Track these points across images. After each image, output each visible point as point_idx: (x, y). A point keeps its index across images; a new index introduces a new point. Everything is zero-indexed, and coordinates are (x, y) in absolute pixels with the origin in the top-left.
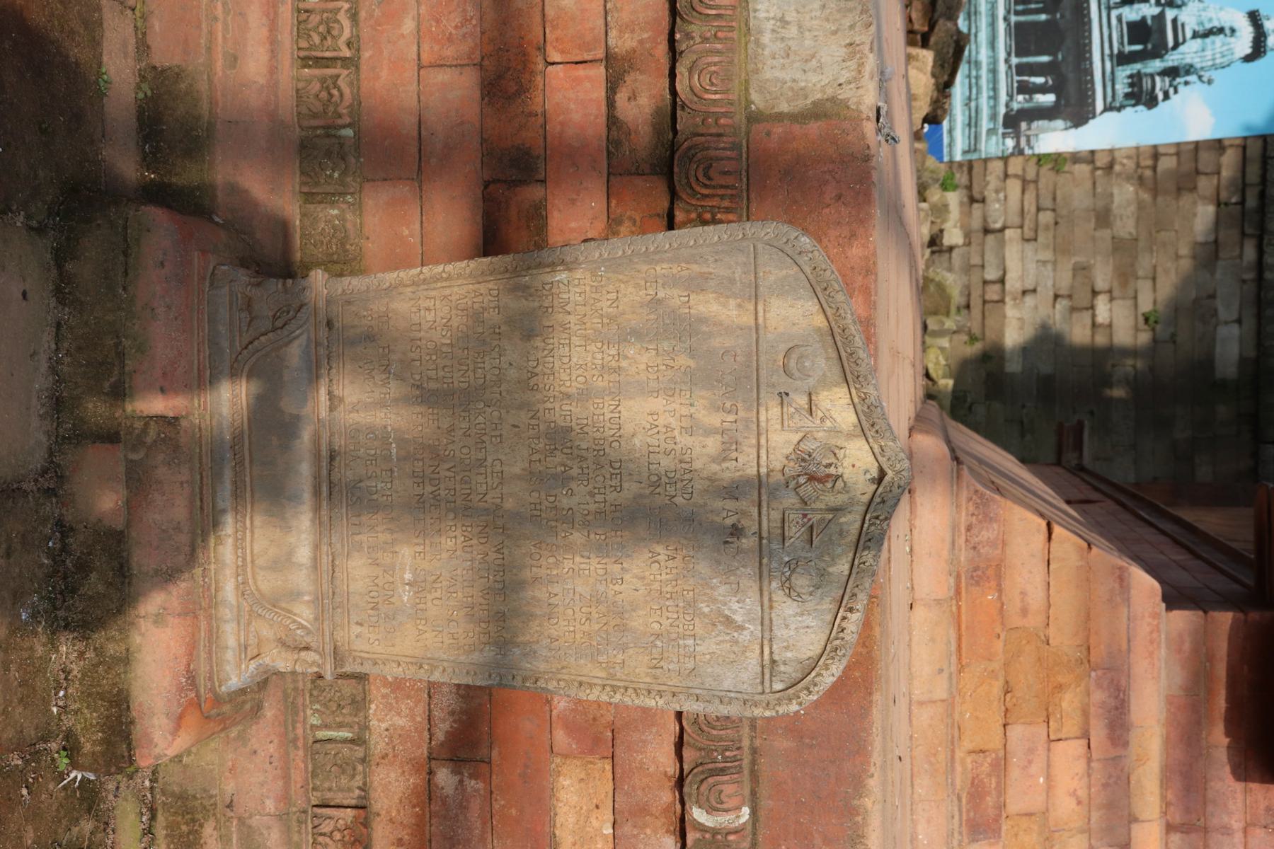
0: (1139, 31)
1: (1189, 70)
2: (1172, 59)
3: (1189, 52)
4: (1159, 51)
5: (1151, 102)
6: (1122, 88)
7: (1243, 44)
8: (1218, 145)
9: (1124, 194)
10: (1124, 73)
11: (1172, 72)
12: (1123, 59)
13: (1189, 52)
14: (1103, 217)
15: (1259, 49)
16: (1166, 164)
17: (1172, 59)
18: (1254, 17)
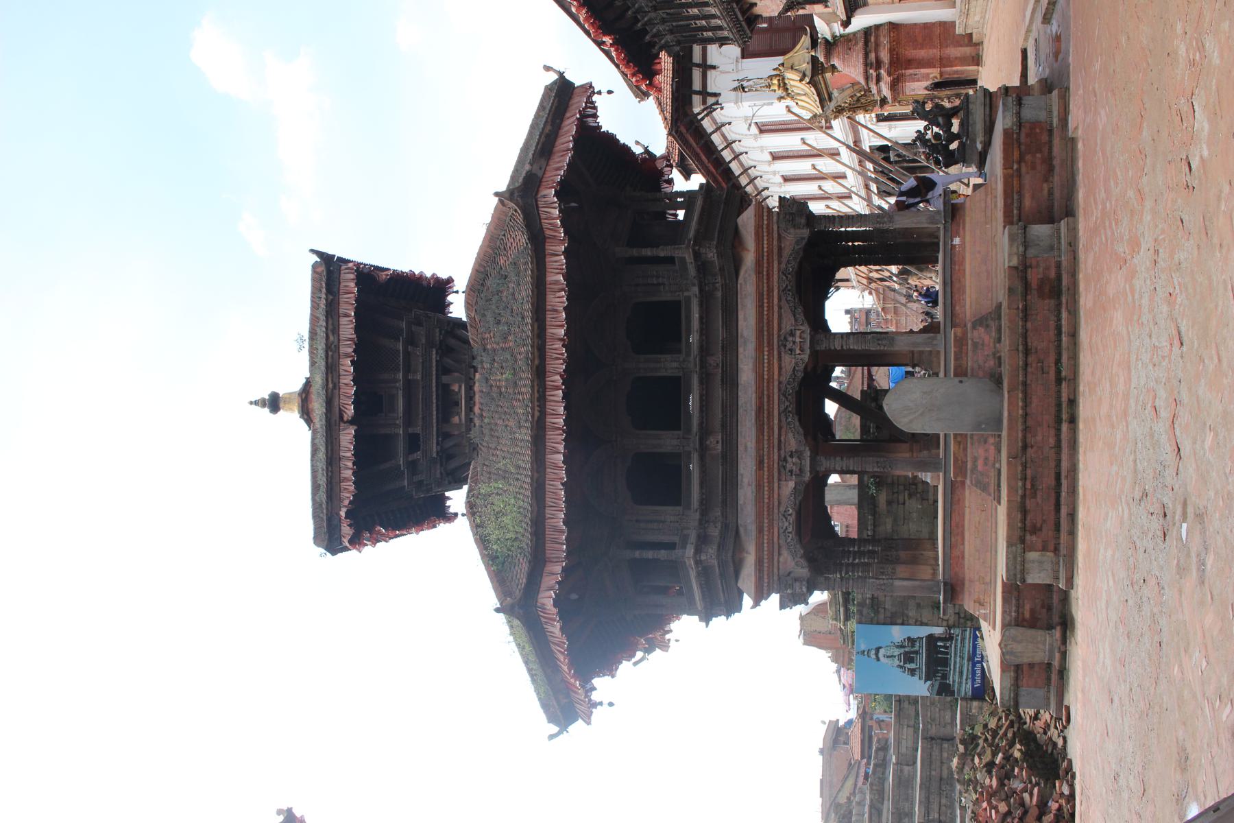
0: (911, 660)
2: (902, 650)
3: (896, 653)
4: (906, 653)
9: (912, 613)
10: (917, 648)
12: (916, 652)
13: (897, 652)
14: (918, 605)
16: (900, 621)
17: (902, 650)
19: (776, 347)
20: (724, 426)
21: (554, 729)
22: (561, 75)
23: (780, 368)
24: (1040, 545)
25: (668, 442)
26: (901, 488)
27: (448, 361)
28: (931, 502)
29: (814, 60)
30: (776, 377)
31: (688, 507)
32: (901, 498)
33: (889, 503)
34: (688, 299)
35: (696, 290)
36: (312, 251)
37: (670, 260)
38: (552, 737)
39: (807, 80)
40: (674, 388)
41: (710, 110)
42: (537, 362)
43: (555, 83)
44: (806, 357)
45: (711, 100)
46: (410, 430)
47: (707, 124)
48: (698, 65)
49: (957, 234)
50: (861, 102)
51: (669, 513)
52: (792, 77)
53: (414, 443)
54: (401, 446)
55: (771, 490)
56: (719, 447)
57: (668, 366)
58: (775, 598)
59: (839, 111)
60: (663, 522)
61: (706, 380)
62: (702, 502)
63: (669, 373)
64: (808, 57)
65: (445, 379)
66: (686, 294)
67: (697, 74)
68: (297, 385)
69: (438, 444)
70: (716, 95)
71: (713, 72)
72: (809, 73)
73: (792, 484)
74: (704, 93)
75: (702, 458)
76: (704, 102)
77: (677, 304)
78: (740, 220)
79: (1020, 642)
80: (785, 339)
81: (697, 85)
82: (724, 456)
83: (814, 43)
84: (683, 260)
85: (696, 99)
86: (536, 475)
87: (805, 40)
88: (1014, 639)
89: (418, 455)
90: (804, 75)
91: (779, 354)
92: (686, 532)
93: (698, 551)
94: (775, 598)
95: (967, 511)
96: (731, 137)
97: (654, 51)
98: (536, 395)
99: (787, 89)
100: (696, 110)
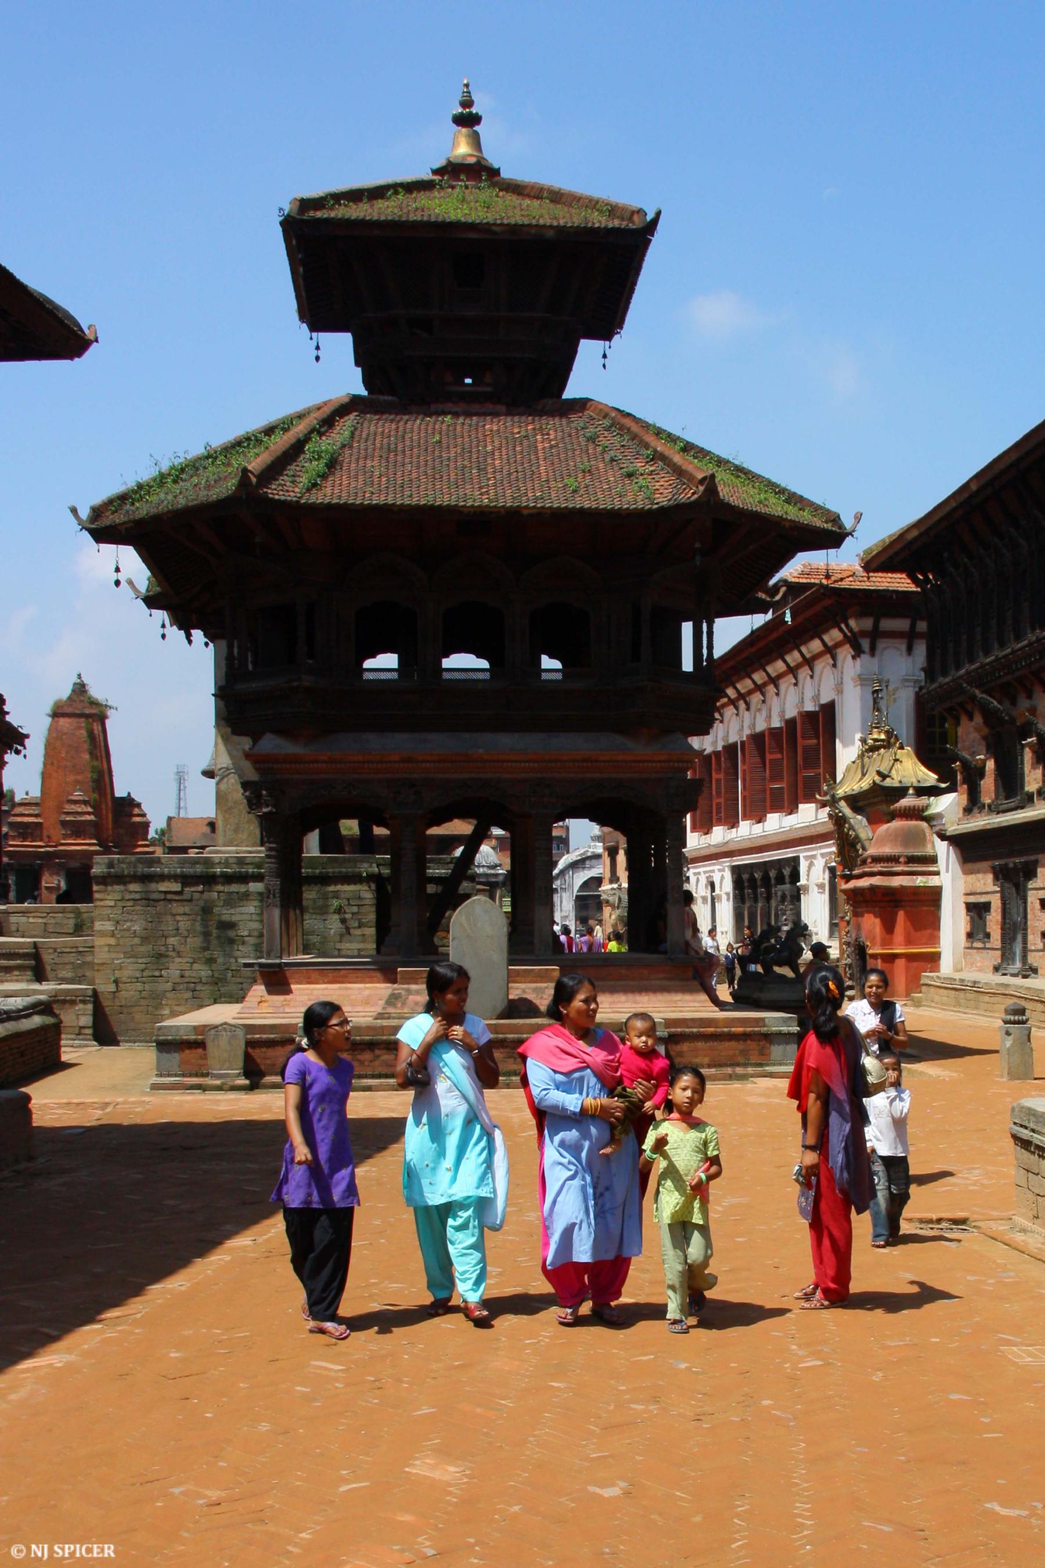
21: (84, 513)
22: (851, 534)
36: (658, 214)
38: (74, 511)
41: (854, 641)
43: (841, 526)
45: (865, 644)
47: (834, 635)
50: (849, 850)
52: (882, 760)
58: (253, 776)
59: (839, 821)
64: (907, 782)
67: (901, 624)
68: (493, 157)
70: (873, 652)
71: (904, 647)
72: (888, 783)
74: (875, 635)
76: (863, 634)
81: (887, 624)
83: (923, 791)
85: (868, 623)
87: (931, 778)
90: (884, 776)
96: (819, 665)
99: (873, 749)
100: (852, 623)
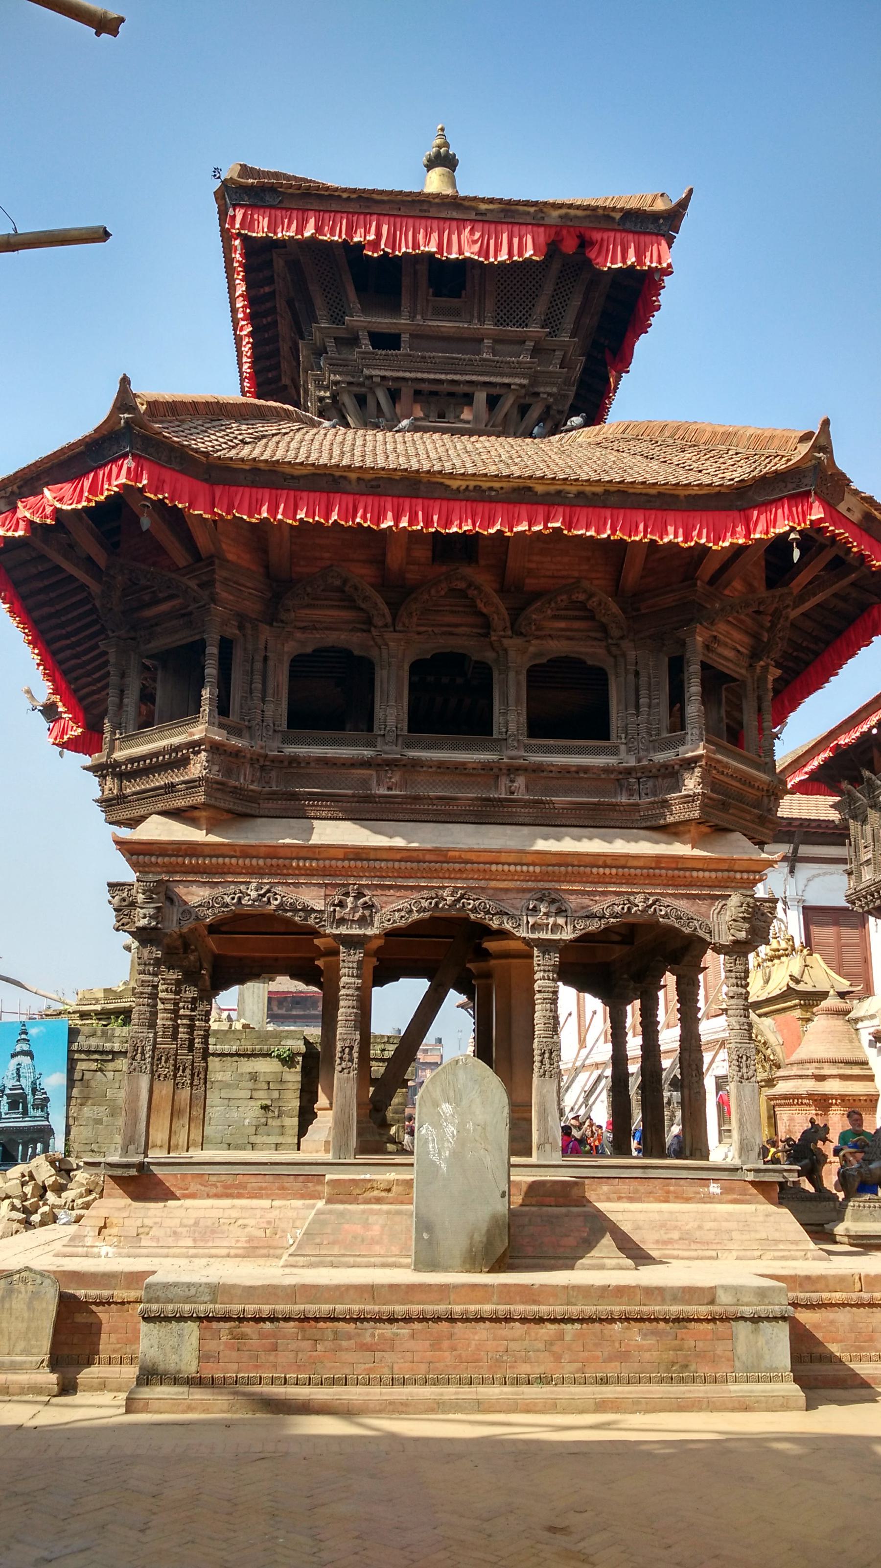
0: (13, 1105)
1: (34, 1083)
2: (28, 1091)
3: (26, 1083)
4: (24, 1096)
5: (47, 1100)
6: (39, 1113)
7: (26, 1060)
8: (71, 1070)
10: (31, 1112)
11: (34, 1090)
12: (25, 1113)
13: (26, 1083)
14: (99, 1121)
15: (29, 1054)
17: (28, 1091)
18: (13, 1056)
19: (541, 885)
20: (417, 798)
23: (507, 890)
24: (212, 1345)
25: (391, 710)
26: (275, 1094)
27: (507, 404)
28: (253, 1139)
29: (824, 995)
30: (493, 884)
31: (286, 740)
32: (256, 1095)
33: (254, 1077)
34: (614, 751)
35: (632, 763)
37: (679, 723)
39: (792, 985)
40: (476, 725)
42: (540, 489)
44: (523, 933)
46: (405, 337)
48: (795, 850)
49: (726, 1191)
51: (277, 709)
53: (386, 341)
54: (383, 322)
55: (311, 873)
56: (383, 791)
57: (510, 715)
60: (263, 701)
61: (490, 773)
62: (294, 761)
63: (497, 719)
65: (481, 397)
66: (623, 748)
69: (383, 378)
71: (786, 870)
72: (800, 987)
73: (319, 905)
75: (366, 764)
77: (607, 737)
78: (738, 835)
79: (30, 1307)
80: (553, 901)
82: (369, 799)
83: (842, 995)
84: (682, 741)
86: (353, 476)
88: (35, 1295)
89: (366, 345)
90: (798, 982)
91: (530, 890)
92: (246, 733)
93: (215, 749)
94: (129, 875)
95: (266, 1203)
97: (845, 785)
98: (485, 485)
